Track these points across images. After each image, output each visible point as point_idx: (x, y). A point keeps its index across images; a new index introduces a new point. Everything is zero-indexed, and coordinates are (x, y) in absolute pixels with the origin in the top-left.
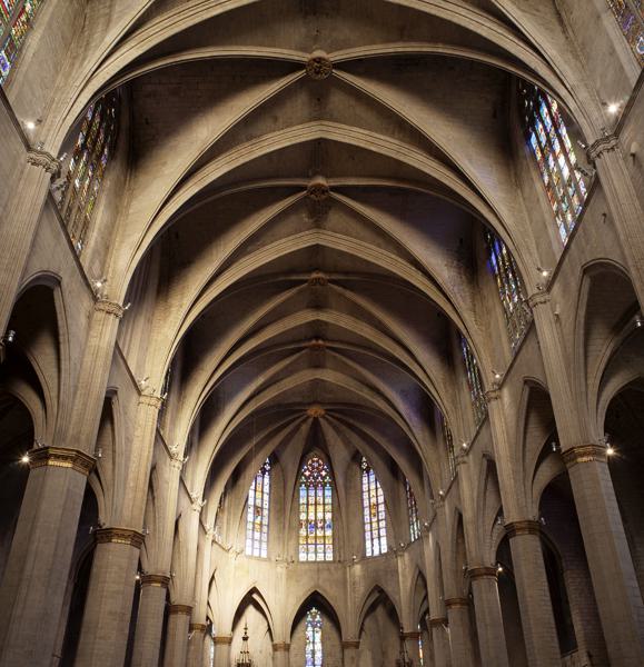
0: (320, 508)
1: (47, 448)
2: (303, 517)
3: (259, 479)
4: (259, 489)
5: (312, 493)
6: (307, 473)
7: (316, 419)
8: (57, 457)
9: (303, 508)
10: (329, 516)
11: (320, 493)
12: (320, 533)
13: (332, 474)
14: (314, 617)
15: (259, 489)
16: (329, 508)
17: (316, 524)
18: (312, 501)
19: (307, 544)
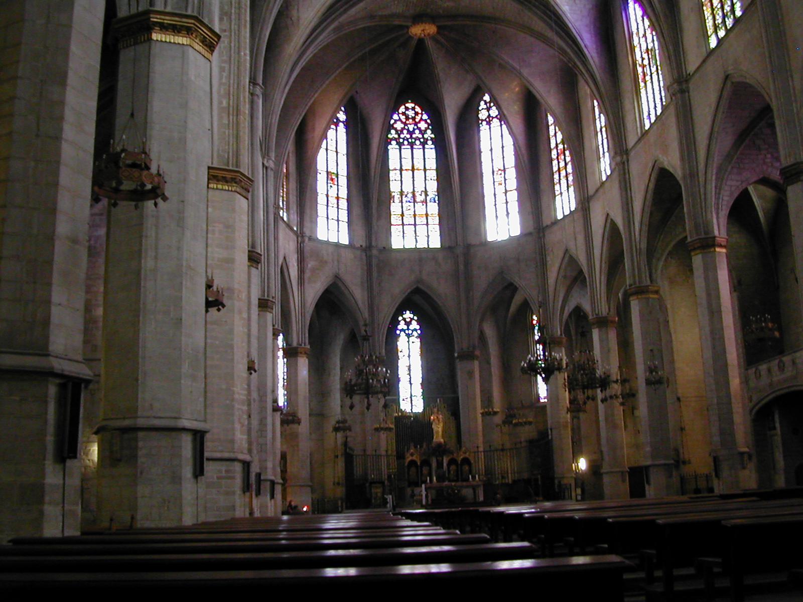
0: (419, 175)
1: (147, 13)
2: (394, 187)
3: (331, 133)
4: (332, 147)
5: (406, 152)
6: (399, 126)
7: (421, 41)
8: (164, 28)
9: (394, 175)
10: (433, 186)
11: (418, 153)
12: (420, 209)
13: (437, 125)
14: (408, 324)
15: (332, 147)
16: (432, 174)
17: (414, 196)
18: (407, 165)
19: (403, 224)
